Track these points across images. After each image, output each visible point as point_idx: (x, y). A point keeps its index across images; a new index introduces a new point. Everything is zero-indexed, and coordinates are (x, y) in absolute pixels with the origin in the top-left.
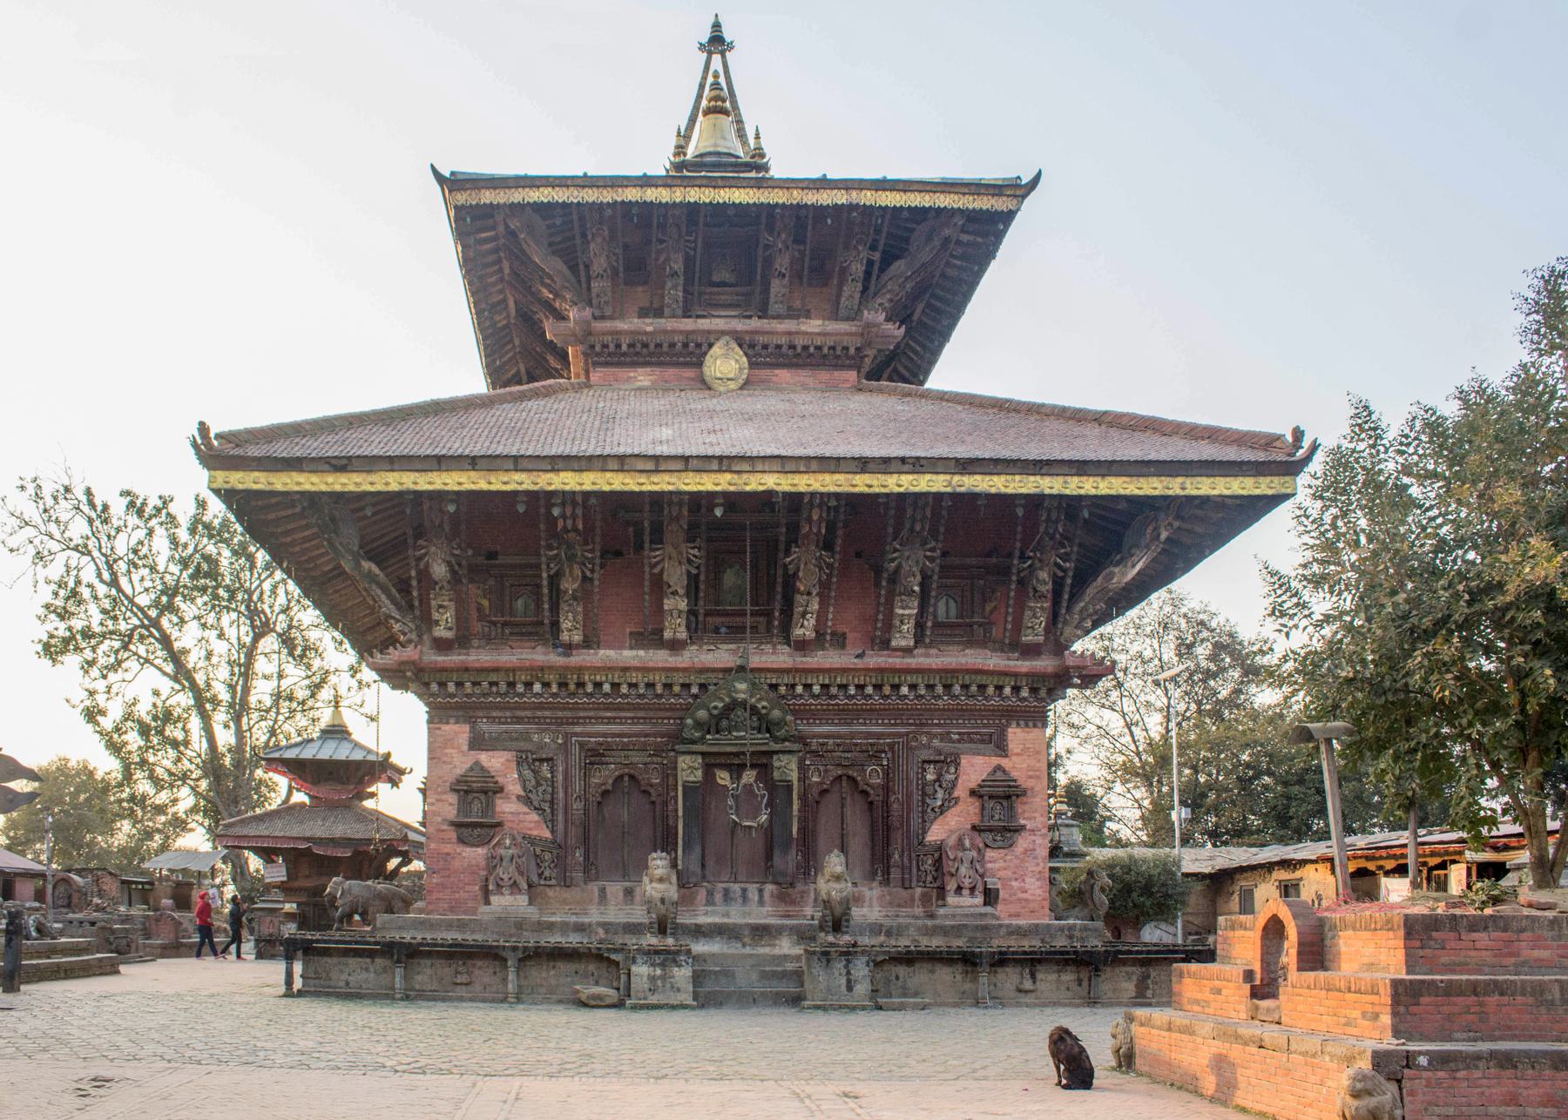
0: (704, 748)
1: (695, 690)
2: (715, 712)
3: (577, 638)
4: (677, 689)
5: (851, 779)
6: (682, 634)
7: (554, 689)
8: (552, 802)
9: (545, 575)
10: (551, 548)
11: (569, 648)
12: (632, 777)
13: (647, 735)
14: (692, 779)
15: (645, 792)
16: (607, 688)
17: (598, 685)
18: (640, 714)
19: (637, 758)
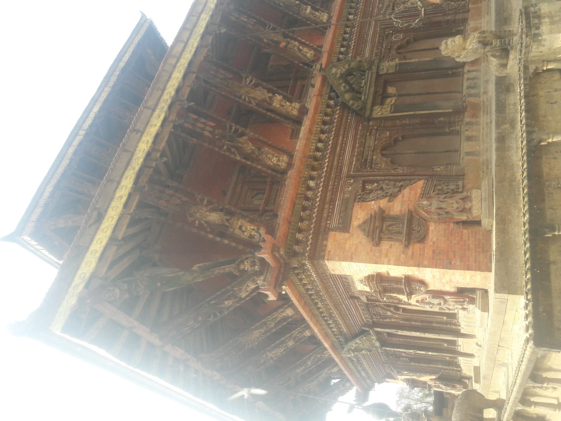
0: (369, 102)
1: (332, 102)
2: (347, 87)
3: (285, 158)
4: (329, 110)
5: (399, 48)
6: (297, 105)
7: (314, 173)
8: (396, 181)
9: (238, 158)
10: (221, 148)
11: (290, 165)
12: (384, 149)
13: (356, 134)
14: (389, 109)
15: (396, 141)
16: (320, 145)
17: (317, 149)
18: (342, 132)
19: (371, 142)
